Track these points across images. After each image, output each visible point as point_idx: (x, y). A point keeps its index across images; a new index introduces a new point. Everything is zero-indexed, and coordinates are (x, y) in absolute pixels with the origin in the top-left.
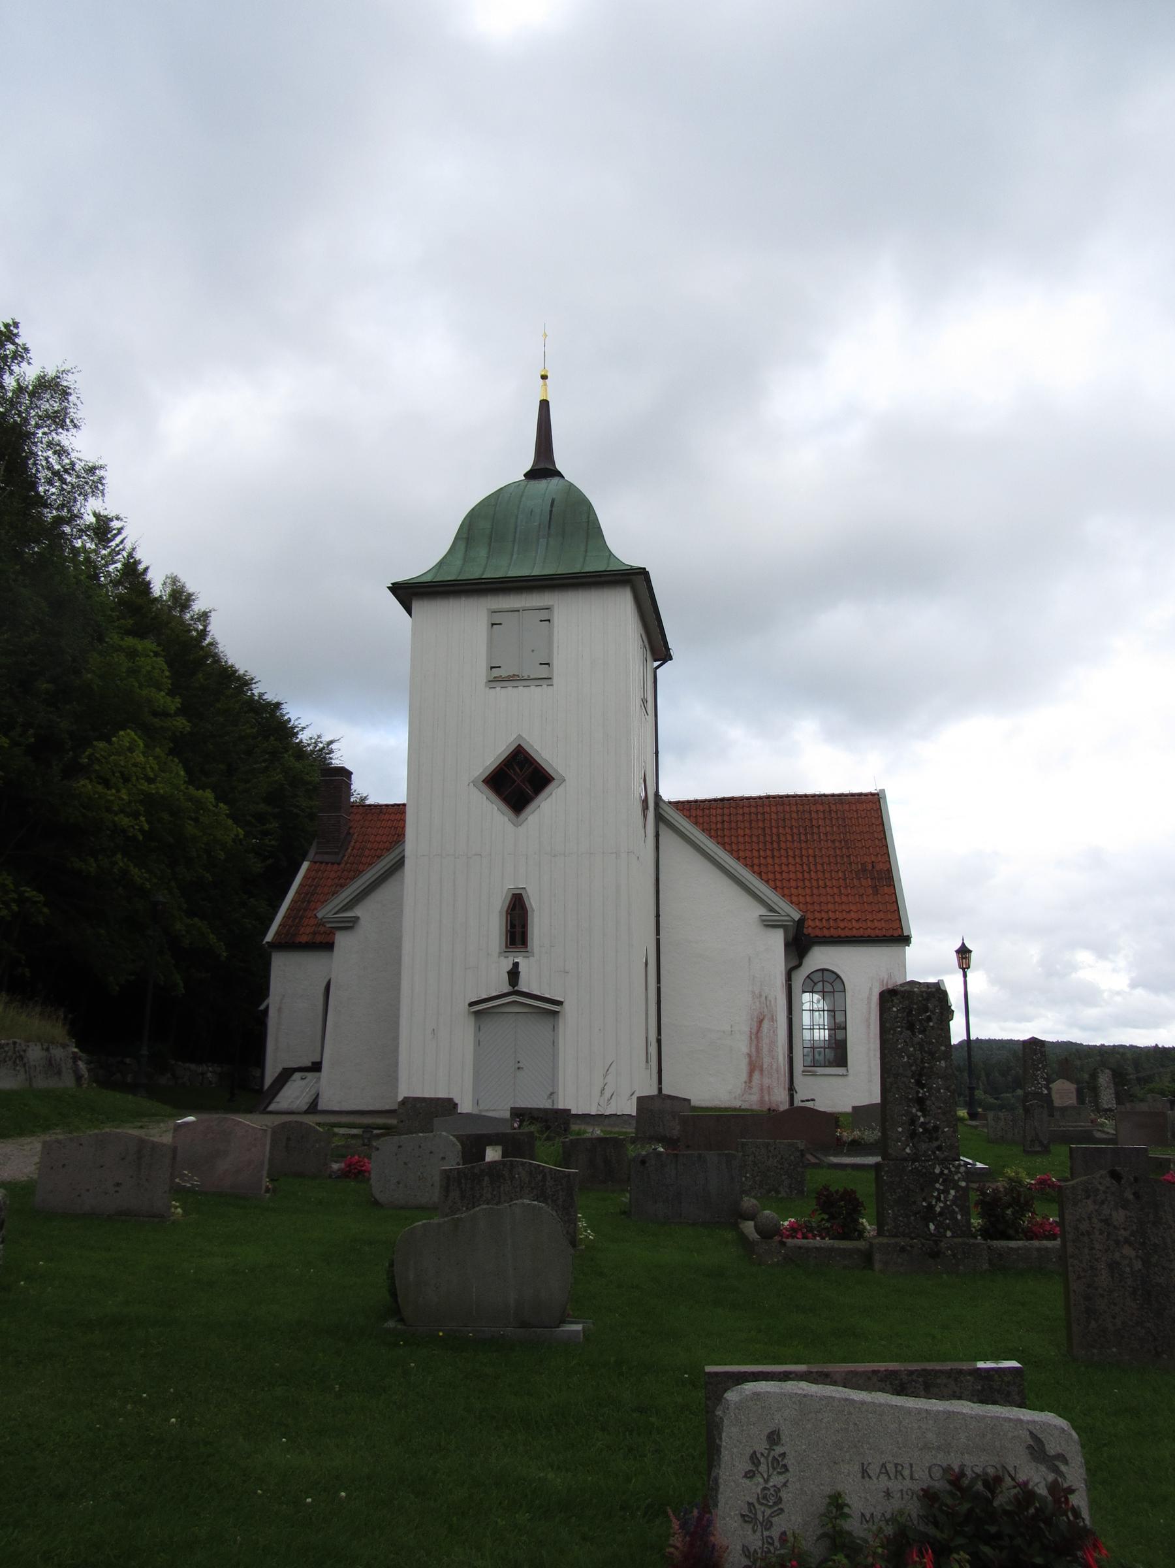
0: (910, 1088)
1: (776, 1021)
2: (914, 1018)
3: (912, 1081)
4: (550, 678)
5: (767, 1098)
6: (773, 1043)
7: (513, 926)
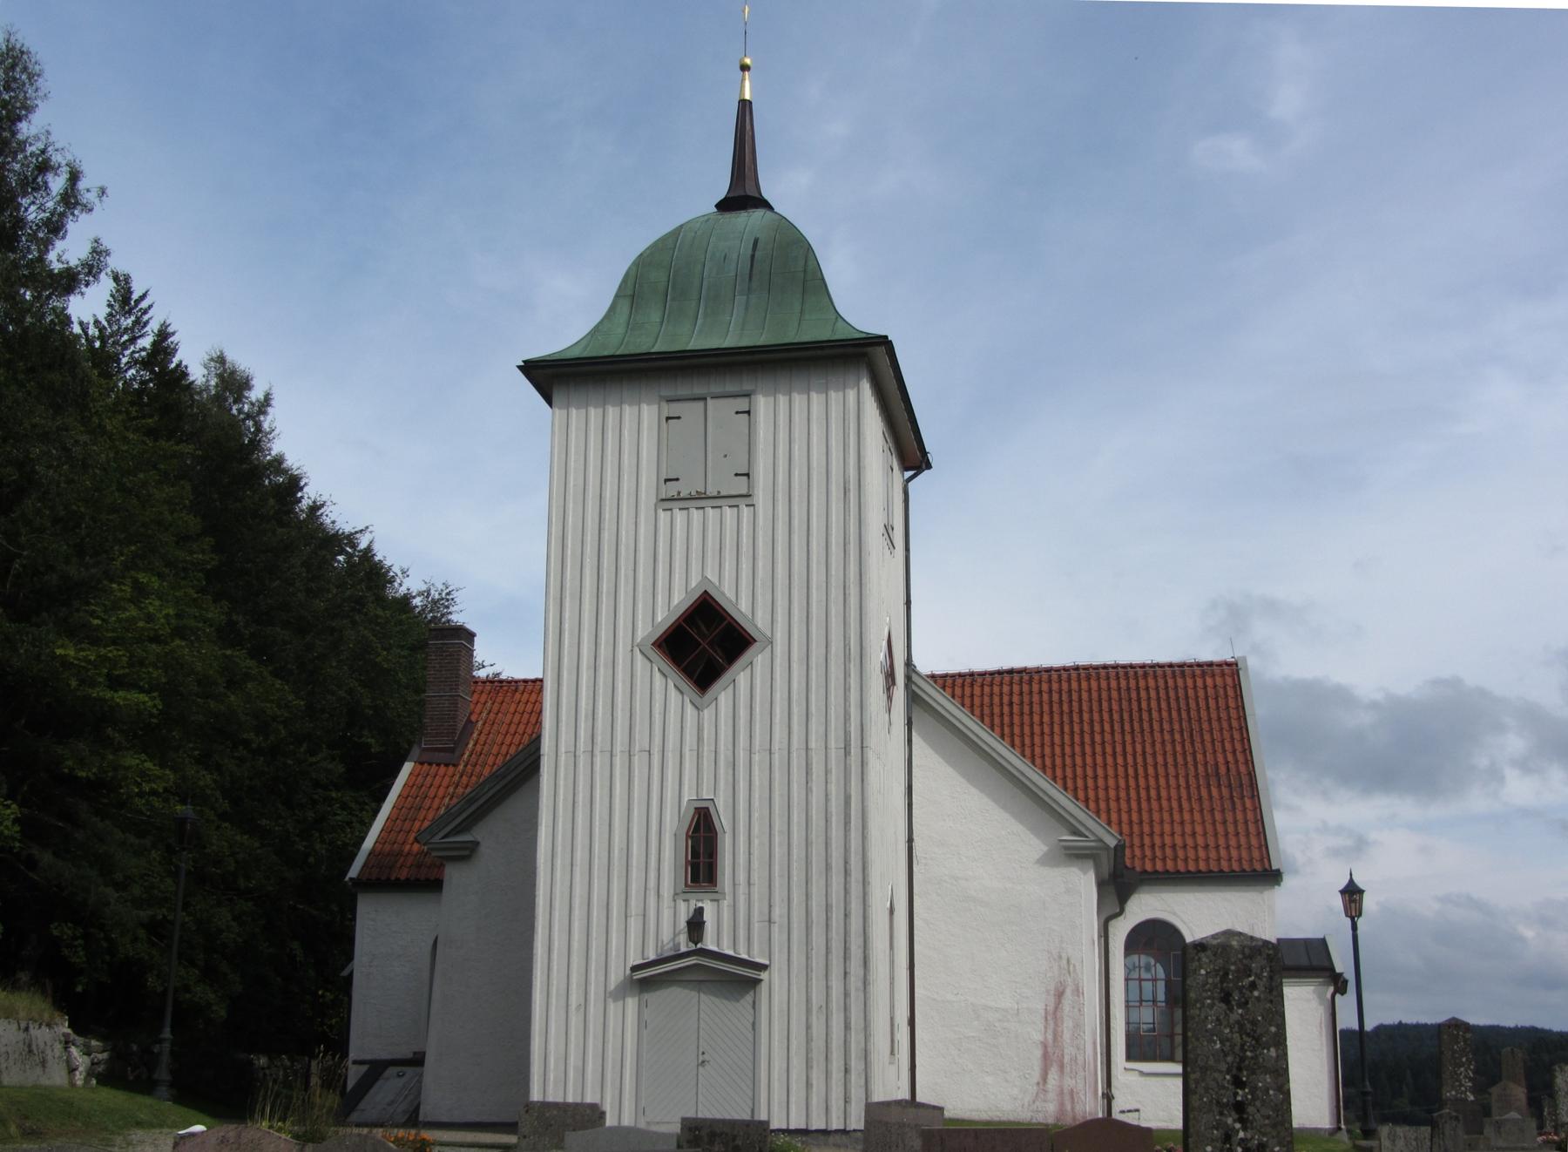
0: (1224, 1087)
1: (1083, 994)
2: (1231, 985)
3: (1228, 1077)
4: (750, 495)
5: (1069, 1107)
6: (1078, 1026)
7: (695, 854)
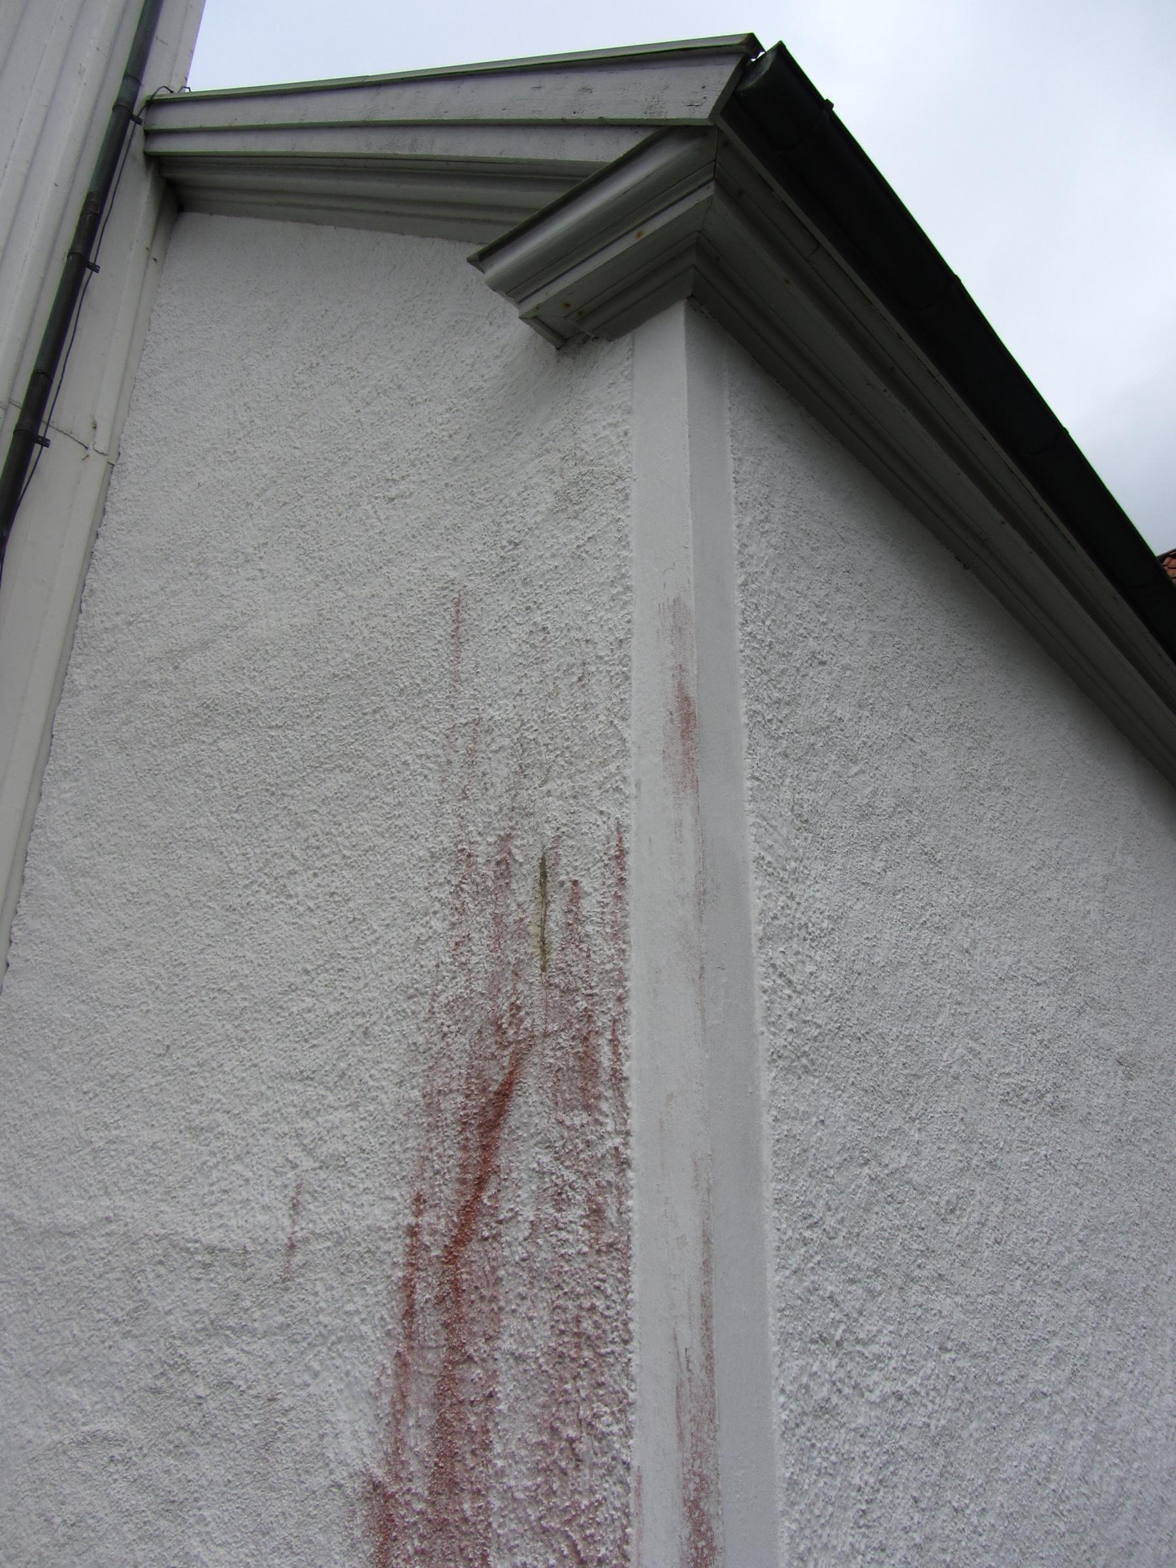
1: (618, 1078)
